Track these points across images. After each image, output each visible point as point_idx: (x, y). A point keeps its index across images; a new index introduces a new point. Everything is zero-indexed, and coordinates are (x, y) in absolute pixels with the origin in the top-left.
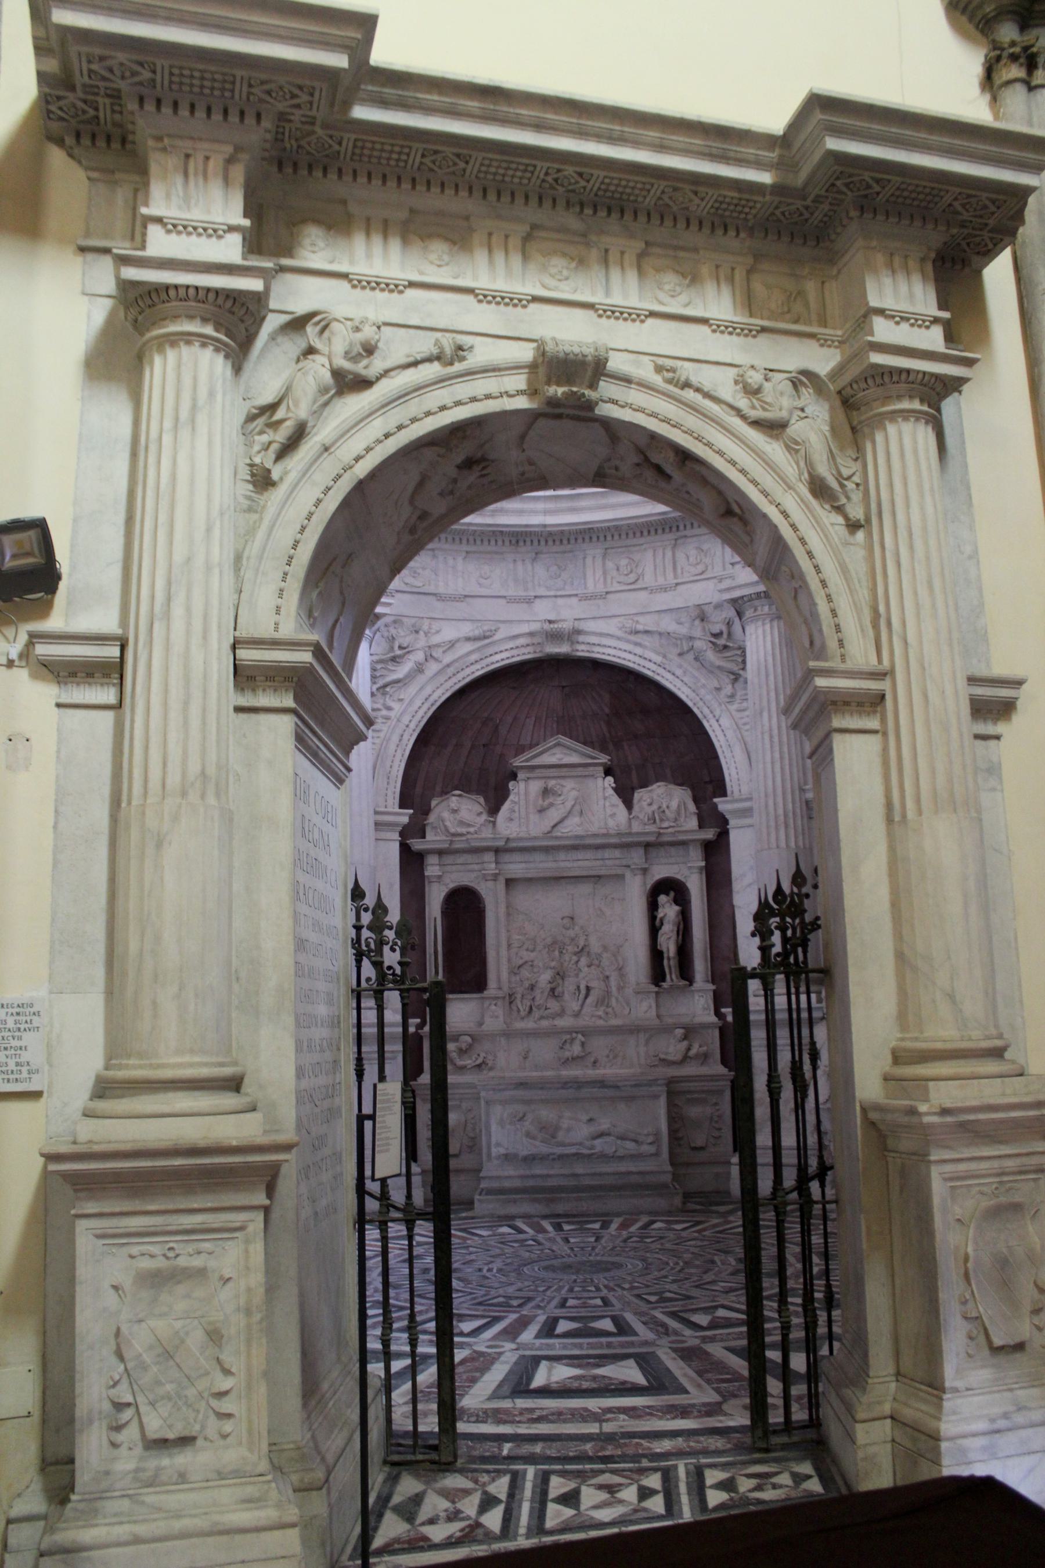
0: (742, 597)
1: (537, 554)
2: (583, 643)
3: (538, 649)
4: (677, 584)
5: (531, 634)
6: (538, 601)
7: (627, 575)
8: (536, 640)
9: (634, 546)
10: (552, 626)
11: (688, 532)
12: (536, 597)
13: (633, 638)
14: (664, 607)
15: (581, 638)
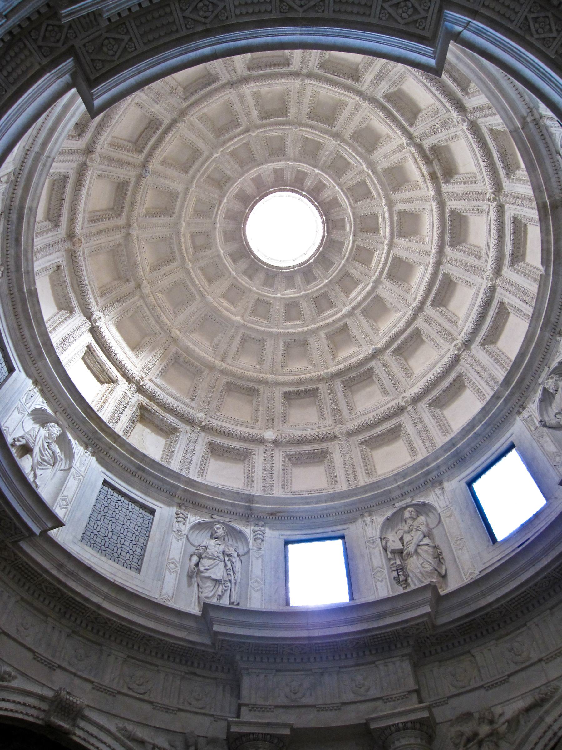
0: (249, 734)
1: (73, 632)
2: (82, 729)
3: (42, 716)
4: (180, 710)
5: (42, 698)
6: (58, 671)
7: (138, 685)
8: (45, 706)
9: (151, 664)
10: (68, 697)
11: (198, 671)
12: (60, 667)
13: (127, 742)
14: (163, 726)
15: (82, 724)
